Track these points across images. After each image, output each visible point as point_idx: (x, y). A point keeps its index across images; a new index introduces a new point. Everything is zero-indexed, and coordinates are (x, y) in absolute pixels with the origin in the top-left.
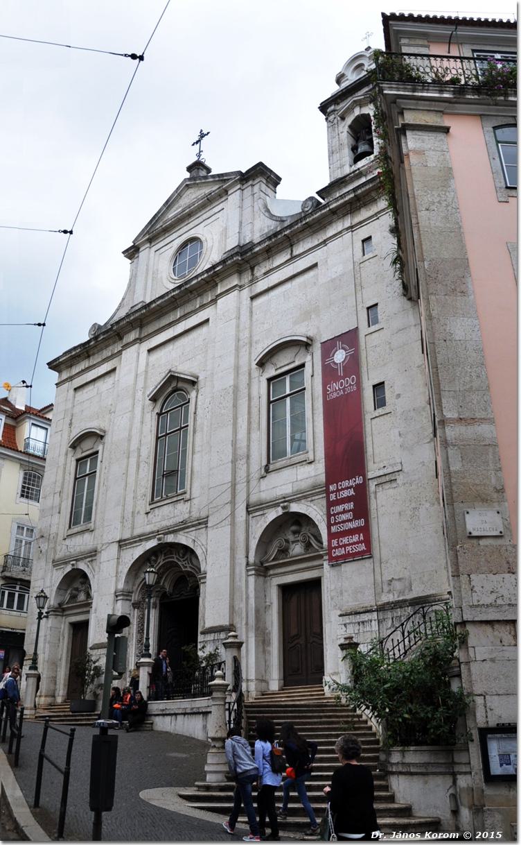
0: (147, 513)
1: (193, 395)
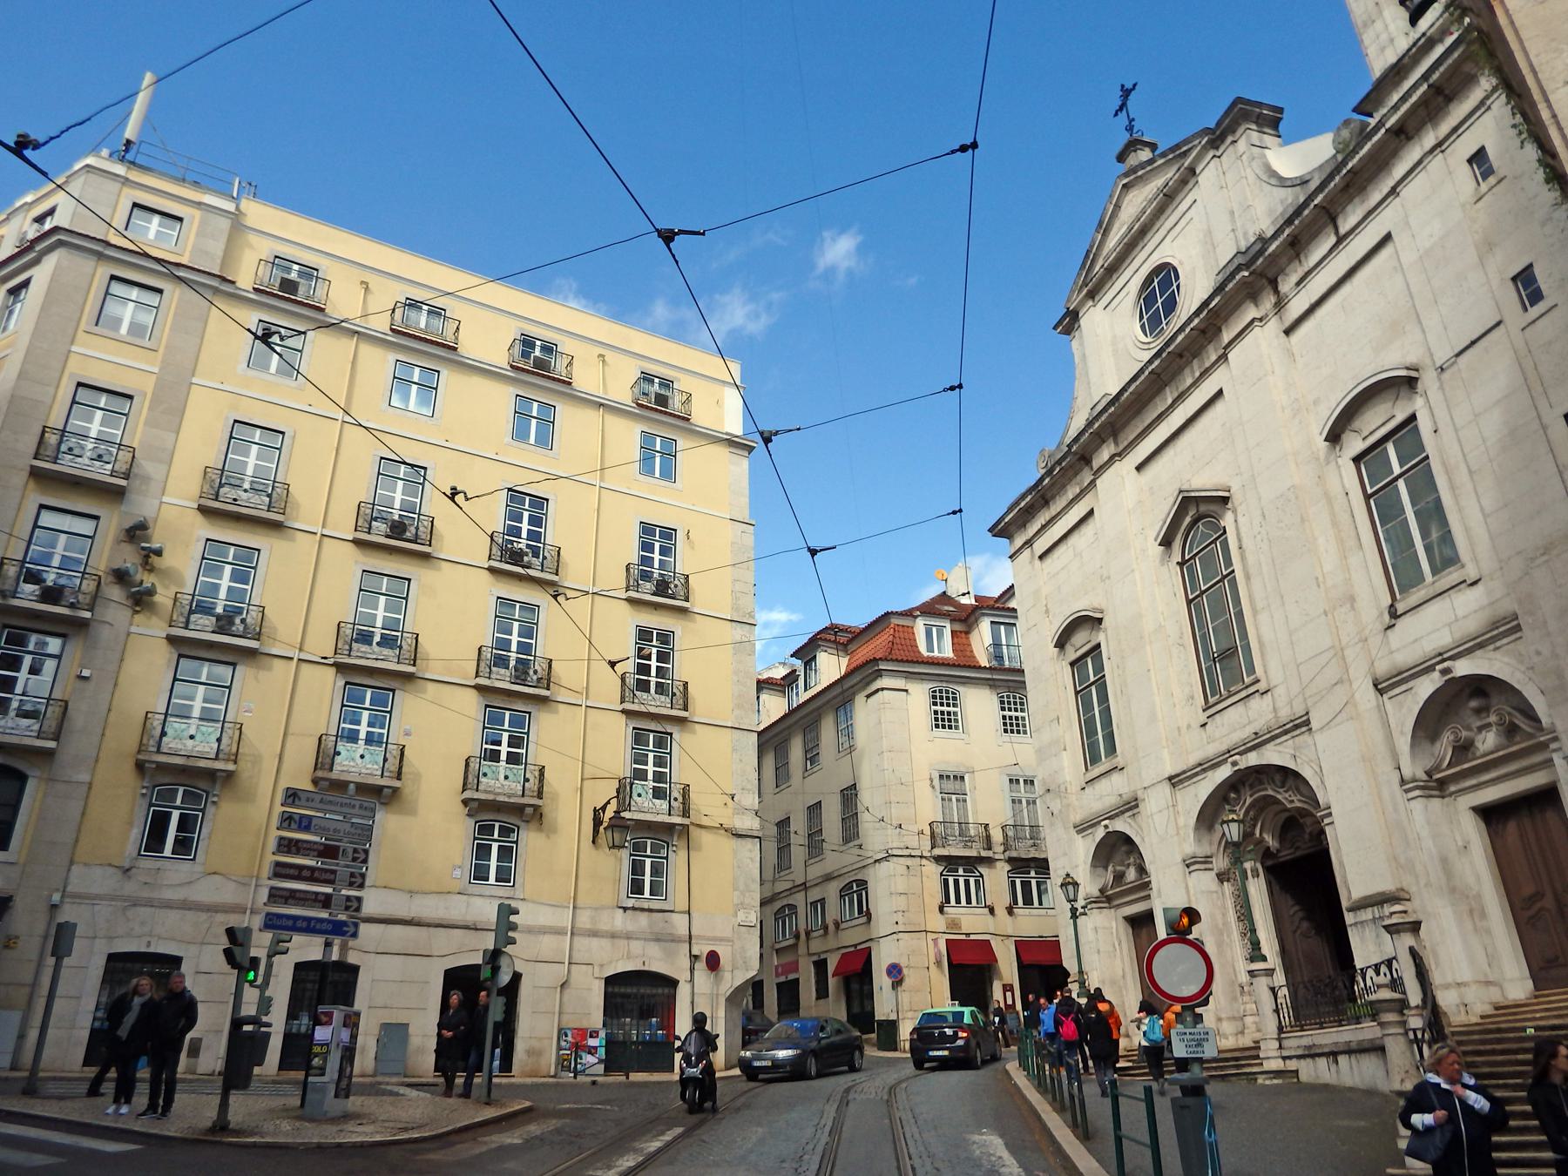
0: (1204, 725)
1: (1227, 521)
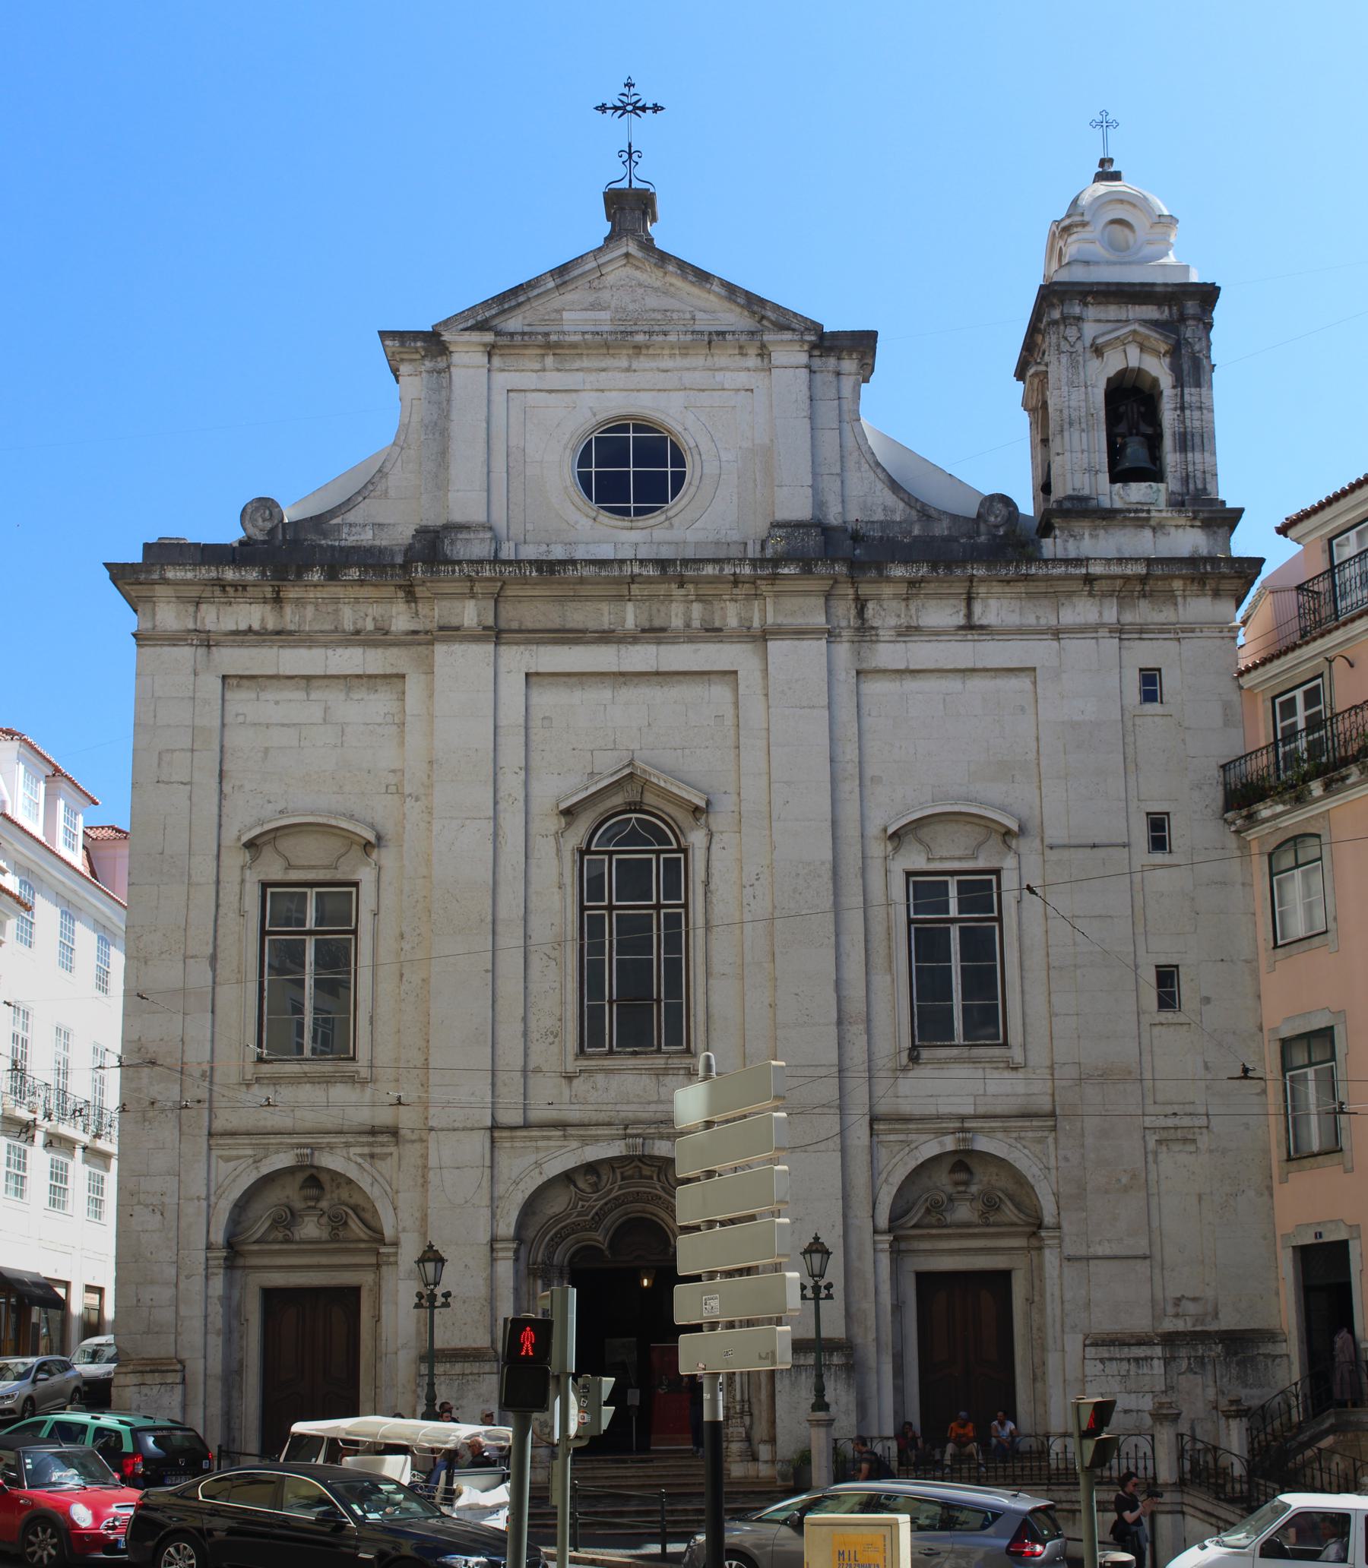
0: (569, 1078)
1: (696, 839)
